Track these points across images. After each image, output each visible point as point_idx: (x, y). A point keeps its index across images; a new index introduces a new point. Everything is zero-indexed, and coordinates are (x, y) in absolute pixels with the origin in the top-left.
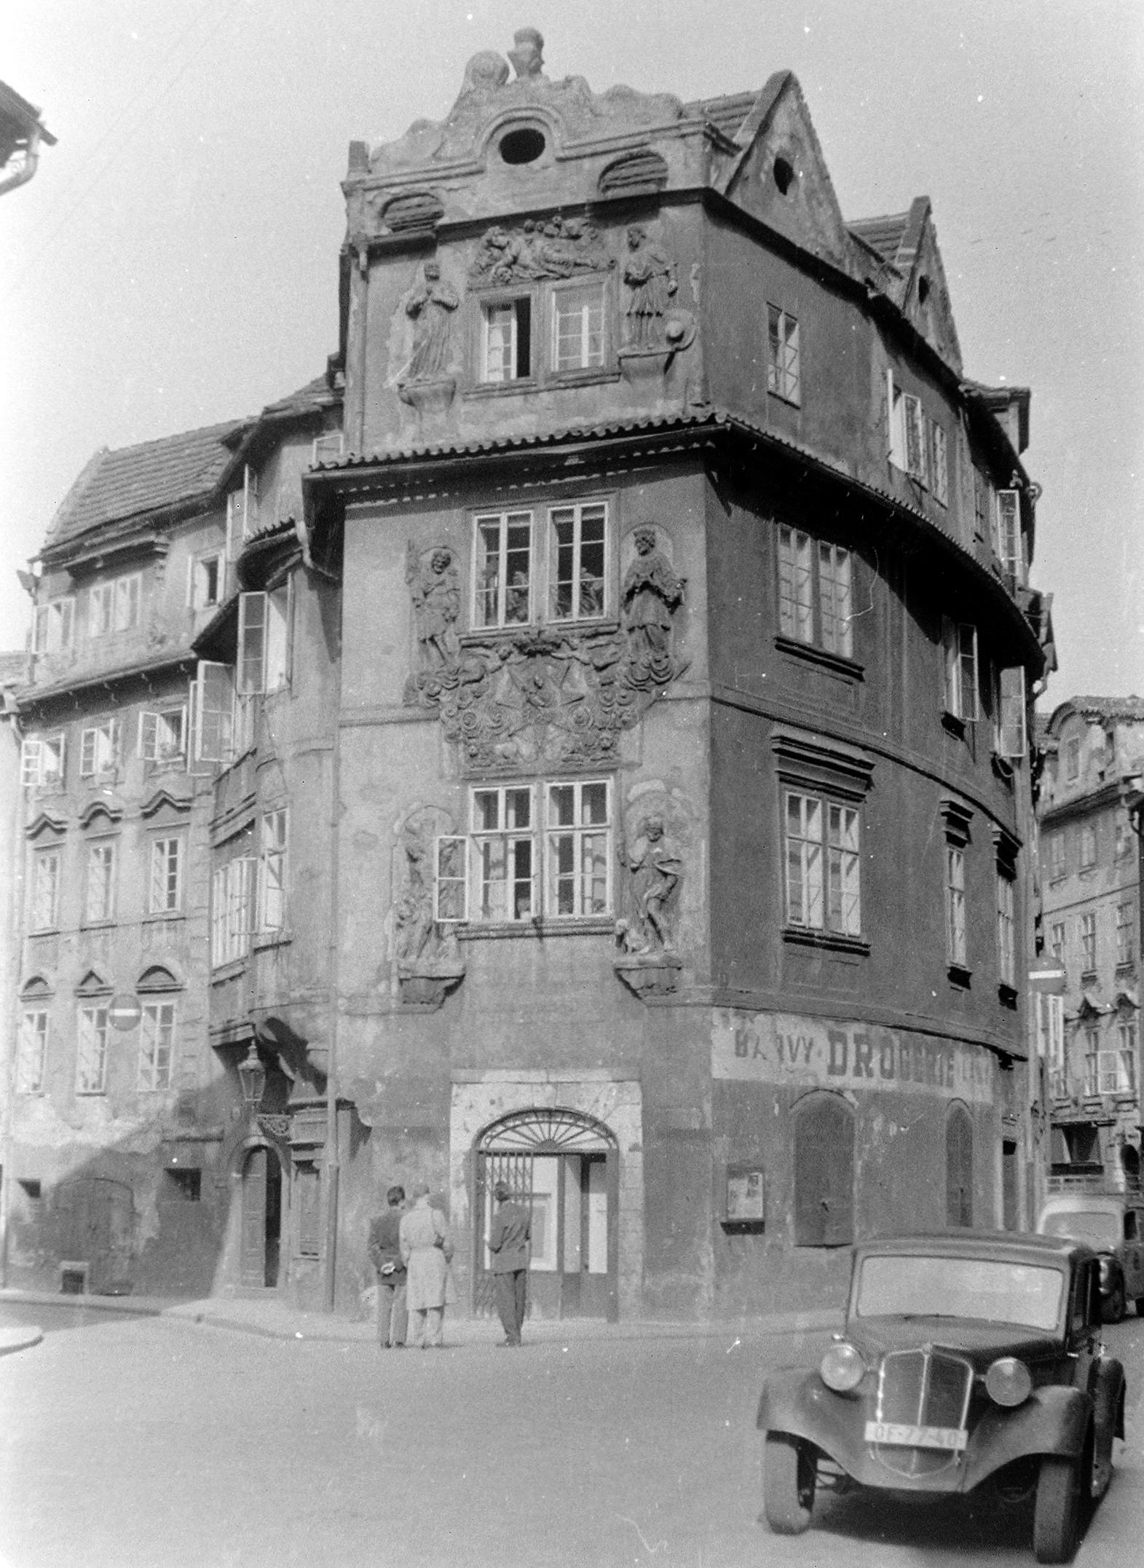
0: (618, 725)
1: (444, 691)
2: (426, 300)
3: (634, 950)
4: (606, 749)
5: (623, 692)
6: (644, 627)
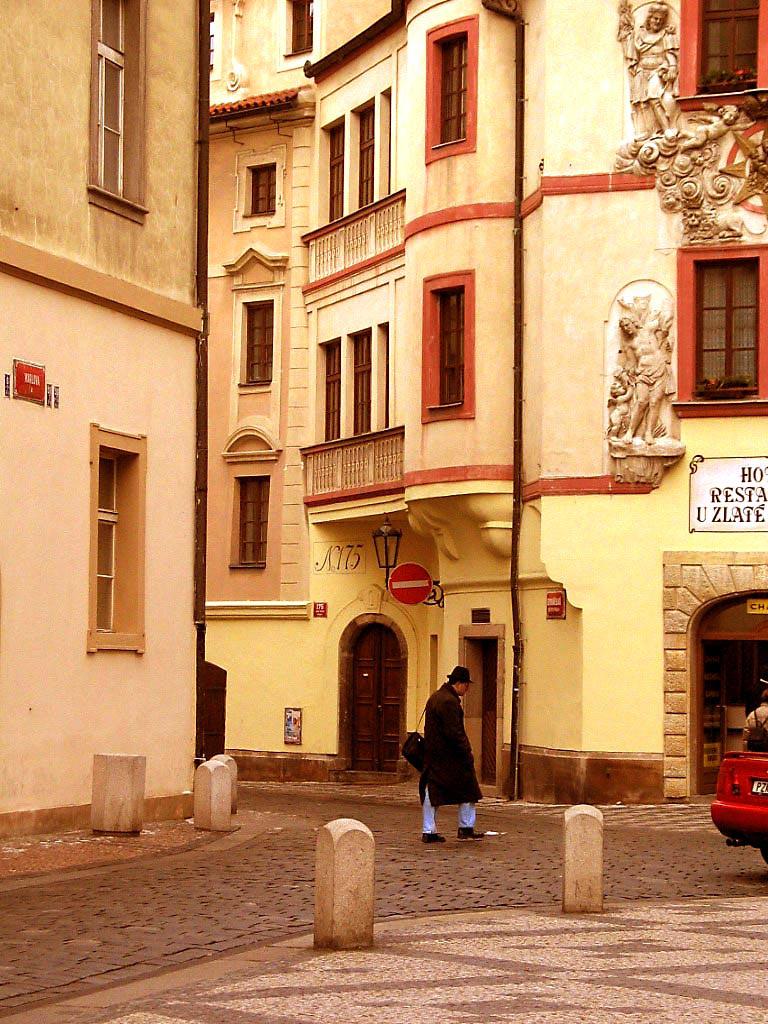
1: (660, 158)
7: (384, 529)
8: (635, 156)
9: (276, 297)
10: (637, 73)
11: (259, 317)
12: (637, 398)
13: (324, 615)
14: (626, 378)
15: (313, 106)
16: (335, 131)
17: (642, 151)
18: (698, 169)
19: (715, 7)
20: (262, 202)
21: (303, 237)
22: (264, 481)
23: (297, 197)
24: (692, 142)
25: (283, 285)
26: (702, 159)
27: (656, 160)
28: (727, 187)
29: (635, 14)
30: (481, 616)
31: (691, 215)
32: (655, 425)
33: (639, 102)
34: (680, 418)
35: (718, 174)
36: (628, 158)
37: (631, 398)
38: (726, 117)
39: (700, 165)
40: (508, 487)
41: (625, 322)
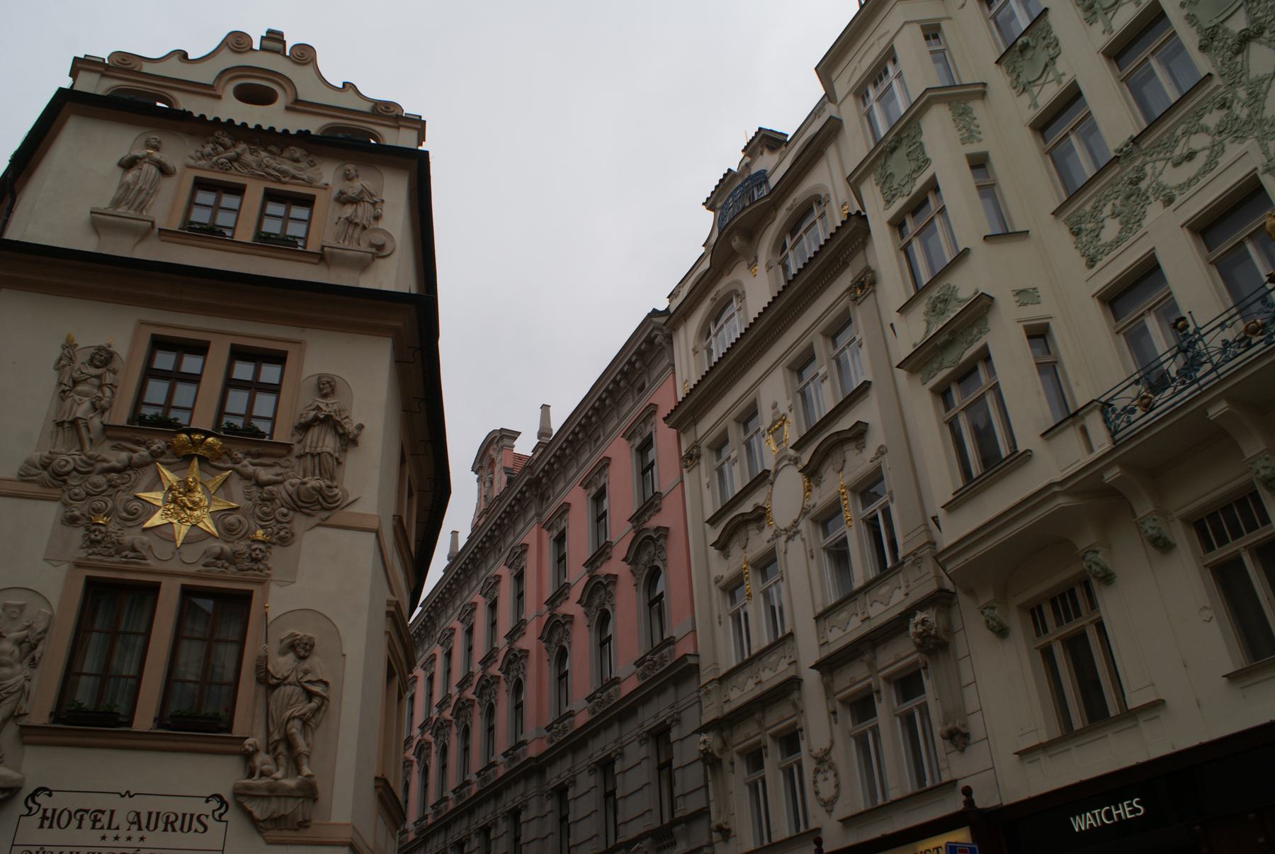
0: (274, 540)
1: (74, 473)
2: (144, 157)
3: (262, 774)
4: (256, 560)
5: (285, 510)
6: (319, 454)
8: (45, 467)
10: (67, 397)
18: (111, 491)
24: (114, 463)
26: (118, 481)
27: (68, 473)
28: (140, 512)
29: (77, 354)
31: (95, 531)
33: (63, 422)
35: (132, 498)
36: (36, 467)
38: (154, 447)
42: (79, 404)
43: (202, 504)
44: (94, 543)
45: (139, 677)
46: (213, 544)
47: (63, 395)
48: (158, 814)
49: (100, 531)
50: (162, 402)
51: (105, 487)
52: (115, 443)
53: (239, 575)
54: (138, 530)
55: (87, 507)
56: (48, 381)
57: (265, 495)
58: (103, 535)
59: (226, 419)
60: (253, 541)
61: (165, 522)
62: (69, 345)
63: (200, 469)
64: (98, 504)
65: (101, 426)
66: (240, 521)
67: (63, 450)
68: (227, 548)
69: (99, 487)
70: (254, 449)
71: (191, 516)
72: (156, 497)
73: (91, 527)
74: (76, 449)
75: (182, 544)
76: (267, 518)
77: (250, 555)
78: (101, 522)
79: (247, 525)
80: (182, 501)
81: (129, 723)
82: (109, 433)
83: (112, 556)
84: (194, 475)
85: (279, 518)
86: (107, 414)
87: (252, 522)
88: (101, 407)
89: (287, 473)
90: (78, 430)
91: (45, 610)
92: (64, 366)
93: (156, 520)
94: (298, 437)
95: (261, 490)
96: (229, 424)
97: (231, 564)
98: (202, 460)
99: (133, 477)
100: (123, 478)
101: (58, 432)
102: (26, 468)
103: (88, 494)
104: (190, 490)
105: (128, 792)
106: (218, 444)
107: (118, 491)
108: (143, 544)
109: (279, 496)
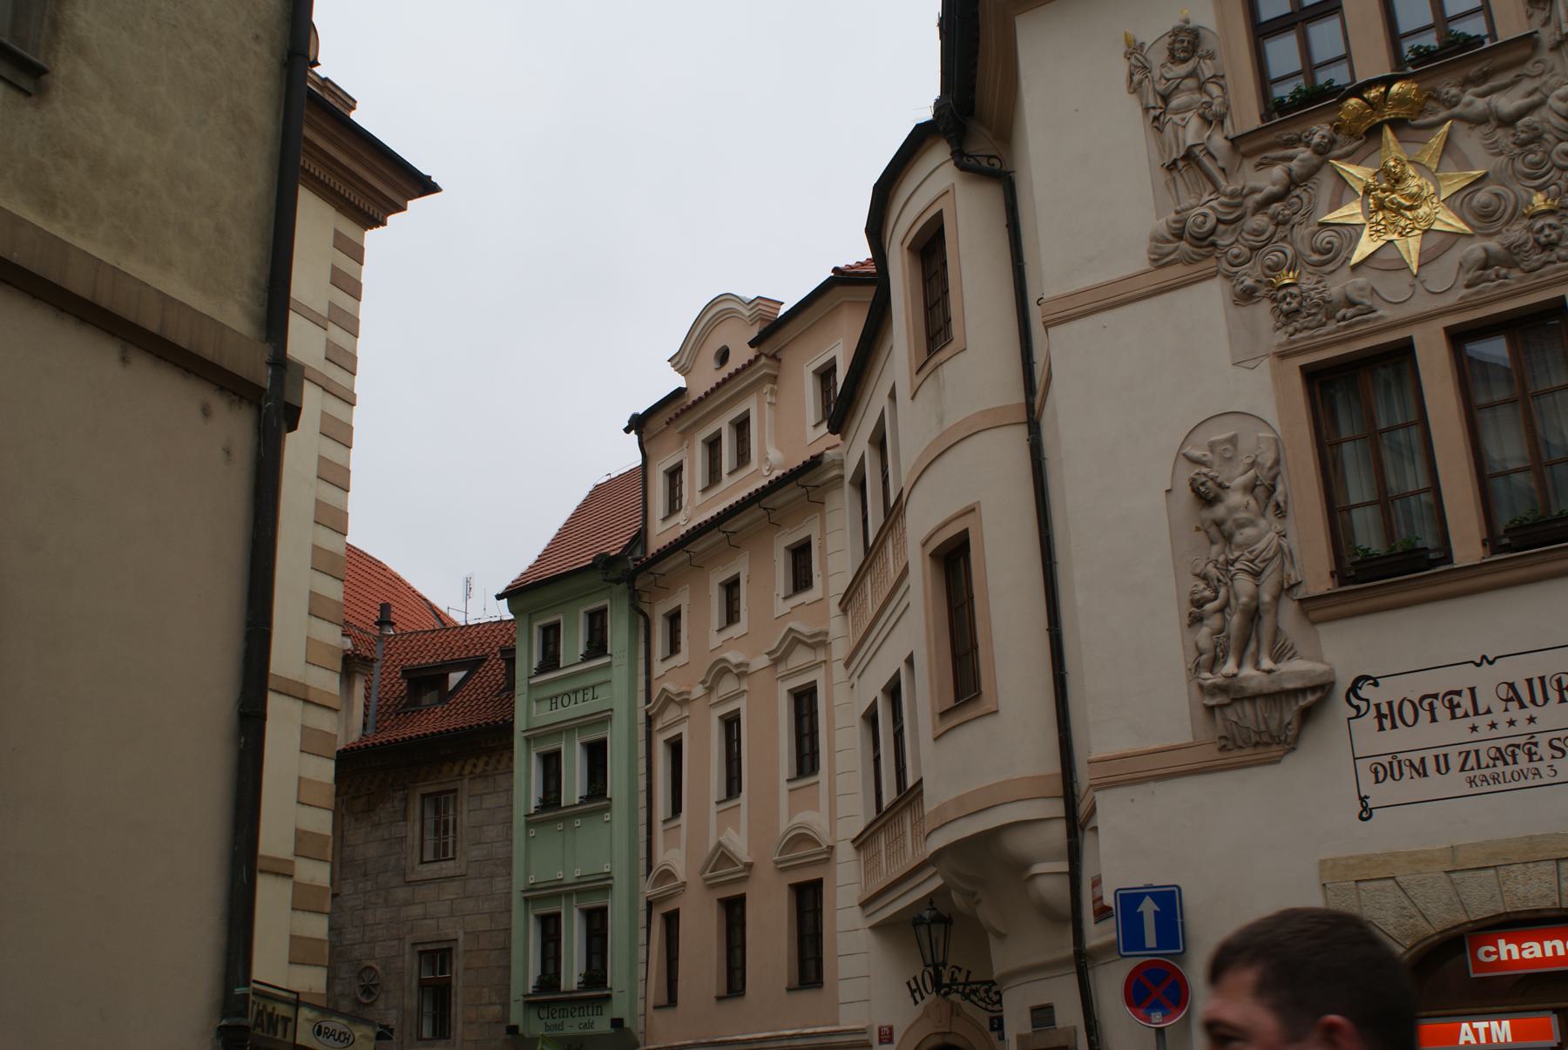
1: (1221, 227)
4: (1549, 246)
7: (927, 914)
8: (1179, 235)
9: (818, 676)
10: (1164, 124)
11: (804, 700)
12: (1237, 598)
13: (890, 1041)
14: (1211, 570)
15: (841, 465)
16: (860, 483)
17: (1190, 222)
19: (1268, 12)
20: (801, 579)
21: (840, 604)
22: (817, 885)
23: (834, 563)
24: (1270, 189)
25: (825, 662)
26: (1286, 212)
27: (1213, 231)
28: (1336, 245)
29: (1150, 56)
30: (1043, 1015)
31: (1284, 297)
32: (1274, 641)
33: (1174, 163)
34: (1314, 623)
35: (1316, 228)
36: (1168, 241)
37: (1227, 604)
38: (1316, 139)
39: (1285, 223)
40: (1058, 808)
41: (1204, 479)
42: (1184, 127)
43: (1425, 194)
44: (1290, 315)
45: (1435, 488)
46: (1468, 249)
47: (1157, 123)
48: (1542, 679)
49: (1291, 295)
50: (1297, 66)
51: (1272, 228)
52: (1257, 159)
53: (1531, 280)
54: (1346, 271)
55: (1259, 268)
56: (1128, 114)
57: (1523, 136)
58: (1298, 299)
59: (1407, 46)
60: (1532, 217)
61: (1380, 243)
62: (1134, 50)
63: (1400, 142)
64: (1273, 258)
65: (1227, 144)
66: (1497, 195)
67: (1193, 201)
68: (1494, 245)
69: (1262, 233)
70: (1473, 71)
71: (1415, 219)
72: (1350, 212)
73: (1276, 294)
74: (1207, 194)
75: (1419, 266)
76: (1544, 170)
77: (1536, 241)
78: (1287, 281)
79: (1512, 196)
80: (1392, 202)
81: (1448, 558)
82: (1243, 149)
83: (1324, 325)
84: (1394, 154)
85: (1561, 162)
86: (1228, 123)
87: (1518, 188)
88: (1215, 115)
89: (1545, 83)
90: (1199, 164)
91: (1265, 434)
92: (1140, 83)
93: (1366, 246)
94: (1540, 16)
95: (1512, 131)
96: (1415, 50)
97: (1509, 268)
98: (1397, 125)
99: (1304, 196)
100: (1292, 205)
101: (1174, 179)
102: (1157, 247)
103: (1253, 249)
104: (1397, 180)
105: (1484, 657)
106: (1411, 90)
107: (1293, 226)
108: (1362, 289)
109: (1547, 126)
